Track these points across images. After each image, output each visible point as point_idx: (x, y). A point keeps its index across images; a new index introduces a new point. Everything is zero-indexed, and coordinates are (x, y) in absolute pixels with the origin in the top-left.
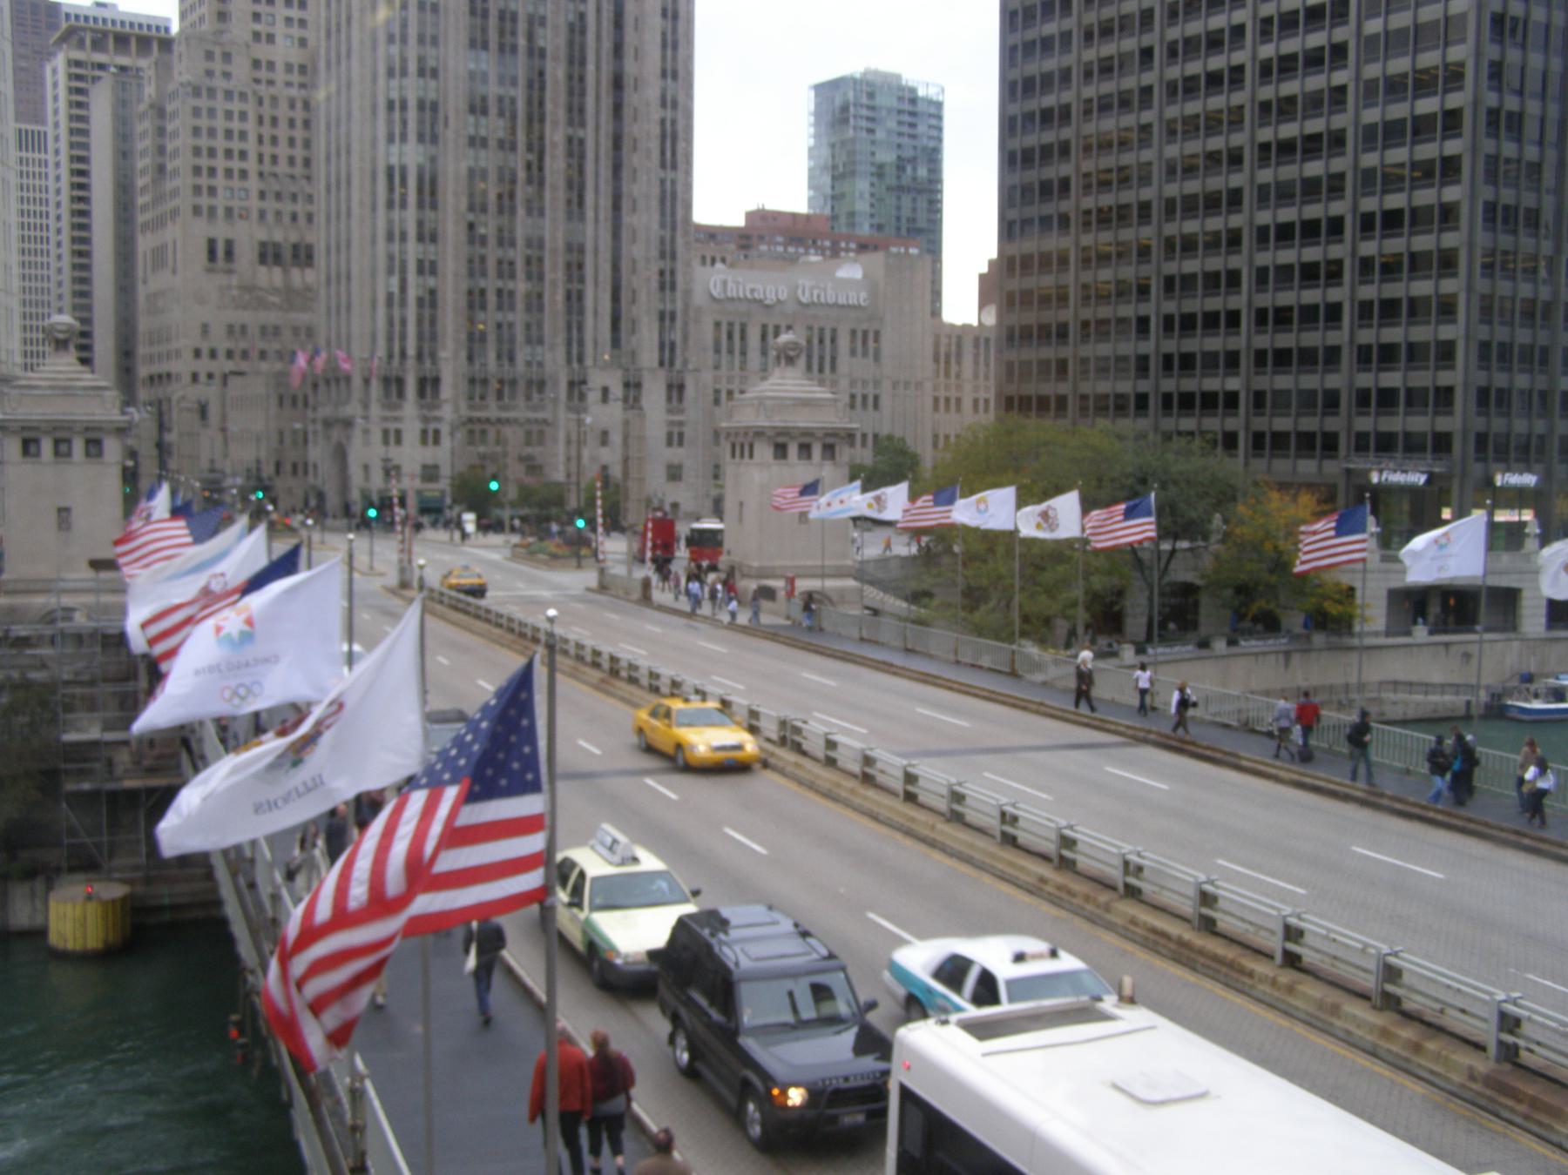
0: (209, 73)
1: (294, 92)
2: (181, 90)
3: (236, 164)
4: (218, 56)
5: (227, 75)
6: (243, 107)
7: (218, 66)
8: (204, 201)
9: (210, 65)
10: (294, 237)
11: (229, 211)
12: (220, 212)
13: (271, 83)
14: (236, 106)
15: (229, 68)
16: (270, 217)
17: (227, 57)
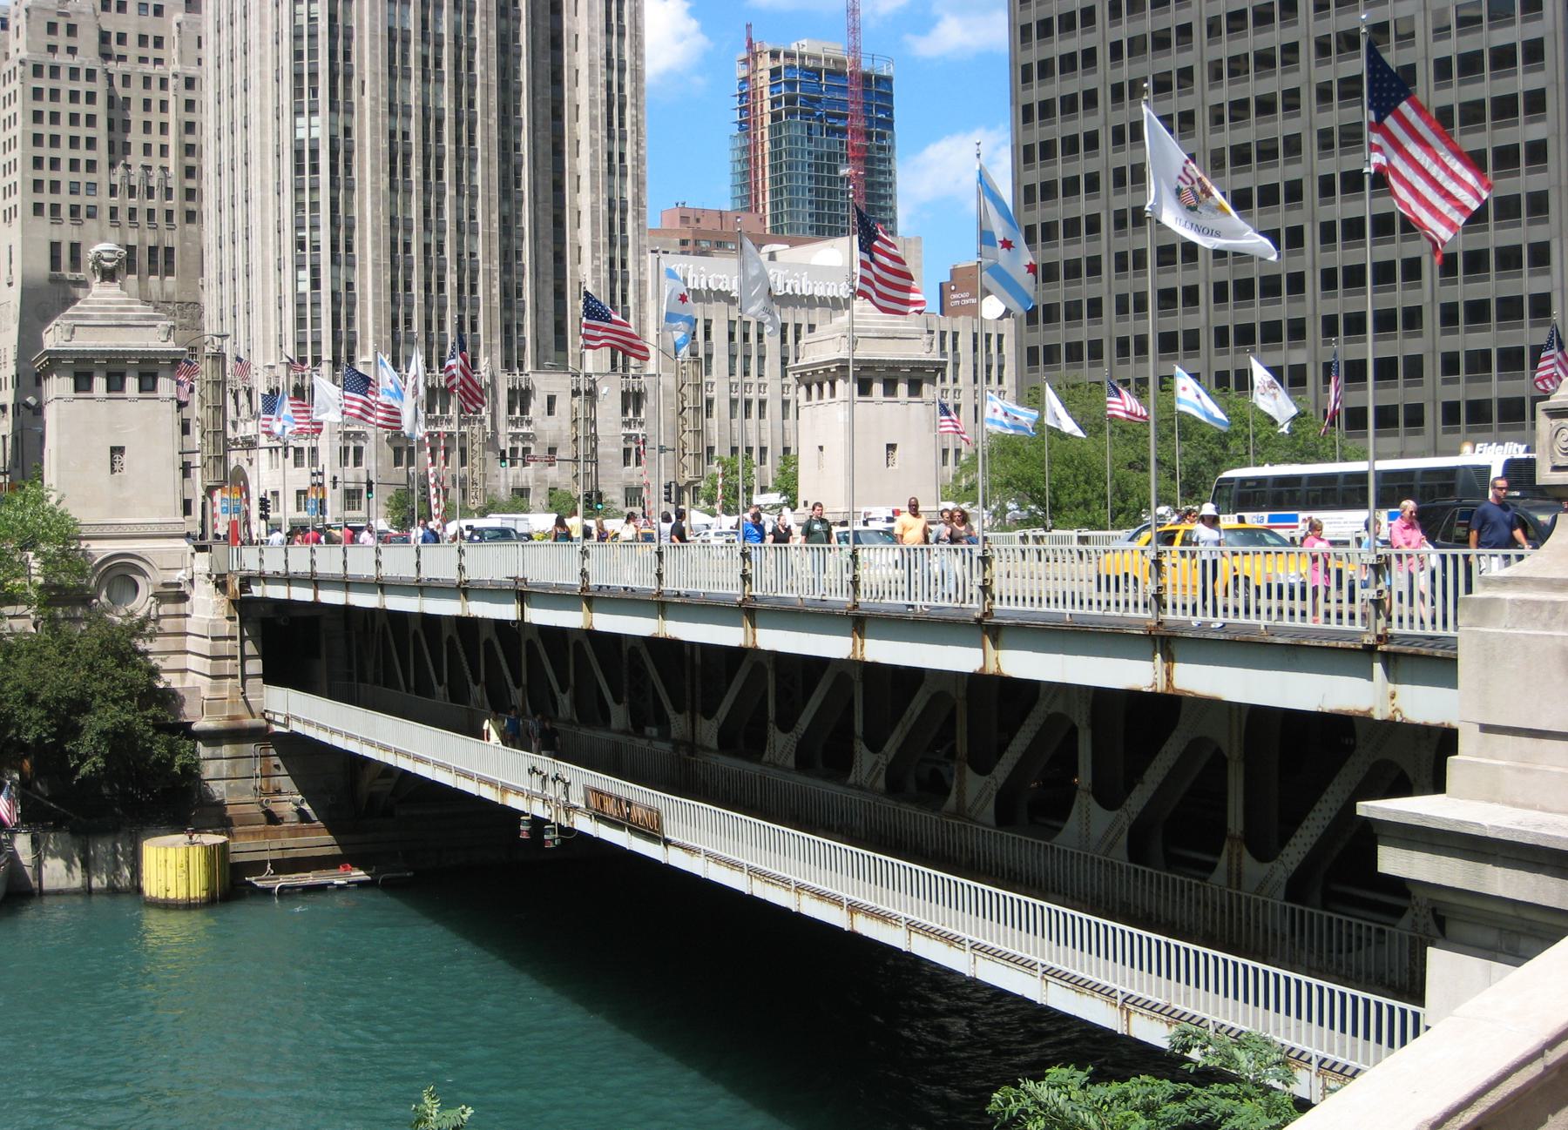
0: (52, 49)
1: (149, 68)
2: (19, 69)
3: (83, 154)
4: (62, 29)
5: (72, 50)
6: (91, 87)
7: (62, 40)
8: (46, 198)
9: (52, 40)
10: (151, 240)
11: (75, 210)
12: (65, 211)
13: (122, 58)
14: (82, 86)
15: (72, 42)
16: (123, 216)
17: (72, 30)
